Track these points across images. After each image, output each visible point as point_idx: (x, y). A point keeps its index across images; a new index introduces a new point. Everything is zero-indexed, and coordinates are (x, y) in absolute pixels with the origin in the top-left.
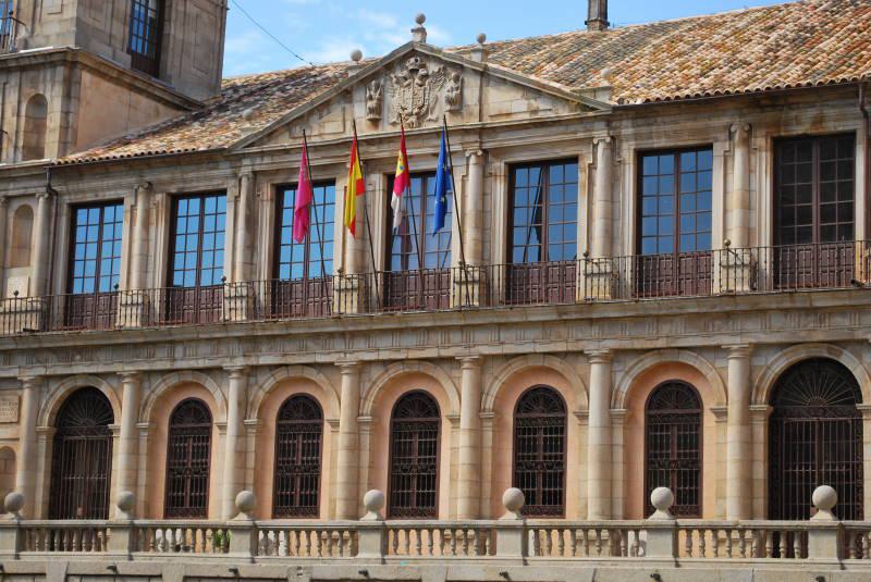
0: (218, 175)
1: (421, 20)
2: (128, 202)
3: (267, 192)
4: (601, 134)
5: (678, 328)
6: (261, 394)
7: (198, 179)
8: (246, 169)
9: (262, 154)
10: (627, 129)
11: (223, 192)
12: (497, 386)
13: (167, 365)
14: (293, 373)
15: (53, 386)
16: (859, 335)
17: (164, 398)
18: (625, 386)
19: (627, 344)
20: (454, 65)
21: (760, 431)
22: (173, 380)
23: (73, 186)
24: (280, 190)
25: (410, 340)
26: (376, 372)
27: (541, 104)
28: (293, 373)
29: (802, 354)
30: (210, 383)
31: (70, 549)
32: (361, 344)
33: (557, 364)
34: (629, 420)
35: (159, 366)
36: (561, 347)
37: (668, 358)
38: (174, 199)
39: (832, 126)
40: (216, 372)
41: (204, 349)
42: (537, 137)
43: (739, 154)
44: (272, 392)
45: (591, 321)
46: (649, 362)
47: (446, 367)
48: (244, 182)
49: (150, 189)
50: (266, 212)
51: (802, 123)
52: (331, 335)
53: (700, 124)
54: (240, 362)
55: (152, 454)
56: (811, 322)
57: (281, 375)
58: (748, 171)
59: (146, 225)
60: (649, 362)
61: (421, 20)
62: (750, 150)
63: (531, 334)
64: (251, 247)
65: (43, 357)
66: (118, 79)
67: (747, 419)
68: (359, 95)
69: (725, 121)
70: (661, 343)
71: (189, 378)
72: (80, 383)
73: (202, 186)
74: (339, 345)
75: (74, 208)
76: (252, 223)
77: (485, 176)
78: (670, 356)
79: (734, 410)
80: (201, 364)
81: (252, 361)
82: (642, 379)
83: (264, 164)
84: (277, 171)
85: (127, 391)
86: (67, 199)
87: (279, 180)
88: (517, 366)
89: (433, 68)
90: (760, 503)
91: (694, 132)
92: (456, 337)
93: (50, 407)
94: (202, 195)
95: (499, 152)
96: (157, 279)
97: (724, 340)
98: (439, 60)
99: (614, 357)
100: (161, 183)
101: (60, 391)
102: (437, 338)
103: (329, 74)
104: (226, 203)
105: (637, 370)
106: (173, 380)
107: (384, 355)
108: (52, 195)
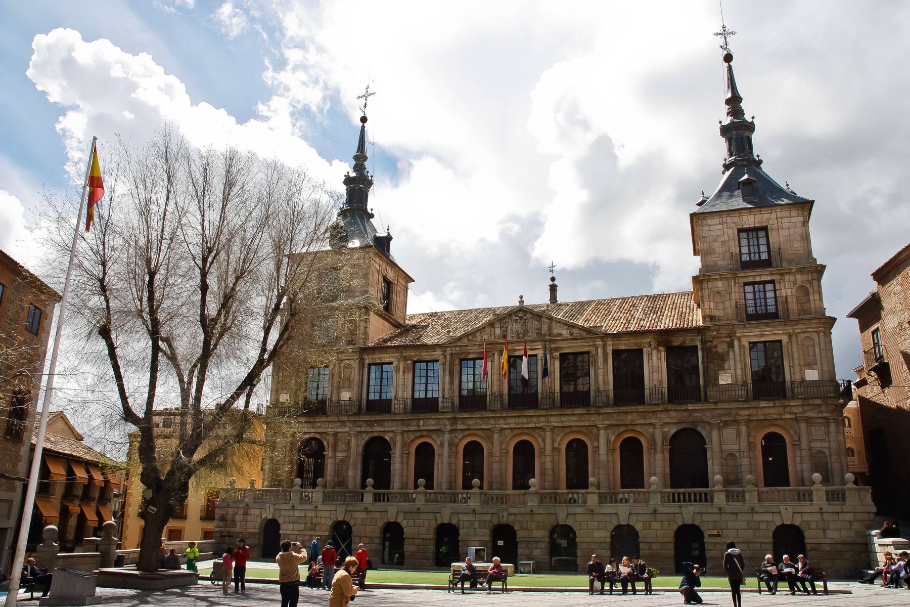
0: (437, 354)
1: (521, 297)
2: (395, 363)
3: (457, 362)
4: (599, 343)
5: (635, 416)
6: (457, 440)
7: (426, 355)
8: (449, 351)
9: (456, 347)
10: (610, 342)
11: (438, 361)
12: (559, 438)
13: (416, 428)
14: (473, 432)
15: (364, 435)
16: (705, 419)
17: (412, 441)
18: (612, 438)
19: (614, 422)
20: (537, 315)
21: (667, 455)
22: (419, 434)
23: (370, 356)
24: (461, 360)
25: (522, 420)
26: (508, 432)
27: (575, 331)
28: (471, 432)
29: (683, 426)
30: (434, 436)
31: (380, 501)
32: (502, 421)
33: (584, 430)
34: (614, 451)
35: (412, 428)
36: (587, 424)
37: (630, 428)
38: (415, 362)
39: (688, 343)
40: (439, 431)
41: (432, 422)
42: (574, 343)
43: (655, 352)
44: (462, 438)
45: (599, 414)
46: (622, 429)
47: (538, 431)
48: (448, 357)
49: (405, 359)
50: (457, 368)
51: (677, 341)
52: (489, 418)
53: (638, 341)
54: (449, 427)
55: (407, 464)
56: (686, 414)
57: (467, 433)
58: (659, 359)
59: (404, 373)
60: (622, 429)
61: (521, 297)
62: (659, 352)
63: (574, 418)
64: (451, 383)
65: (359, 424)
66: (380, 315)
67: (663, 452)
68: (497, 325)
69: (648, 340)
70: (628, 422)
71: (425, 433)
72: (376, 434)
73: (428, 358)
74: (492, 422)
75: (370, 365)
76: (451, 374)
77: (553, 358)
78: (630, 427)
79: (659, 447)
80: (432, 428)
81: (454, 427)
82: (617, 436)
83: (454, 350)
84: (462, 353)
85: (399, 438)
86: (367, 362)
87: (462, 357)
88: (568, 430)
89: (529, 315)
90: (668, 482)
91: (635, 344)
92: (543, 419)
93: (363, 443)
94: (427, 362)
95: (557, 349)
96: (409, 394)
97: (653, 421)
98: (531, 313)
99: (607, 427)
100: (410, 356)
101: (367, 438)
102: (535, 419)
103: (447, 316)
104: (436, 365)
105: (617, 433)
106: (419, 434)
107: (512, 426)
108: (362, 361)
